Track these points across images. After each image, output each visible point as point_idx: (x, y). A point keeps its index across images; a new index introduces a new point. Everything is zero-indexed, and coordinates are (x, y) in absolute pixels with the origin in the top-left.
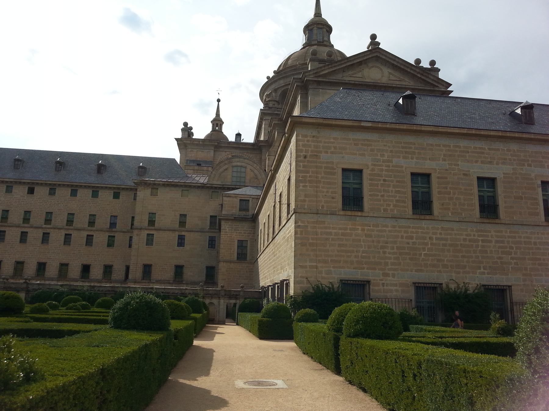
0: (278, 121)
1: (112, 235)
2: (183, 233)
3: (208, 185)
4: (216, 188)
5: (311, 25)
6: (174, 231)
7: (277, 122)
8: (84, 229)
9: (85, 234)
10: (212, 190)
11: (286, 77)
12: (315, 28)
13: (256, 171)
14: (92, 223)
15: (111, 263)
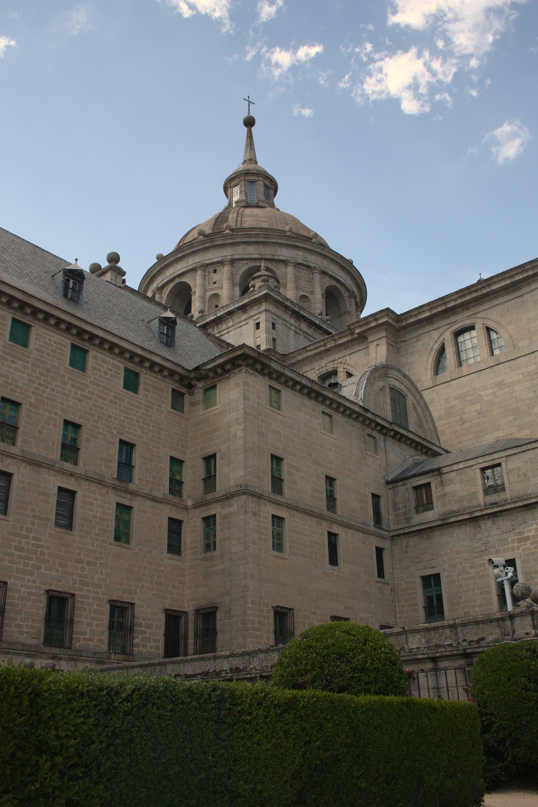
0: (394, 320)
1: (126, 502)
2: (335, 529)
3: (369, 415)
4: (377, 424)
5: (253, 174)
6: (319, 517)
7: (390, 321)
8: (49, 466)
9: (53, 482)
10: (368, 431)
11: (264, 243)
12: (261, 183)
13: (419, 410)
14: (70, 449)
15: (126, 598)
